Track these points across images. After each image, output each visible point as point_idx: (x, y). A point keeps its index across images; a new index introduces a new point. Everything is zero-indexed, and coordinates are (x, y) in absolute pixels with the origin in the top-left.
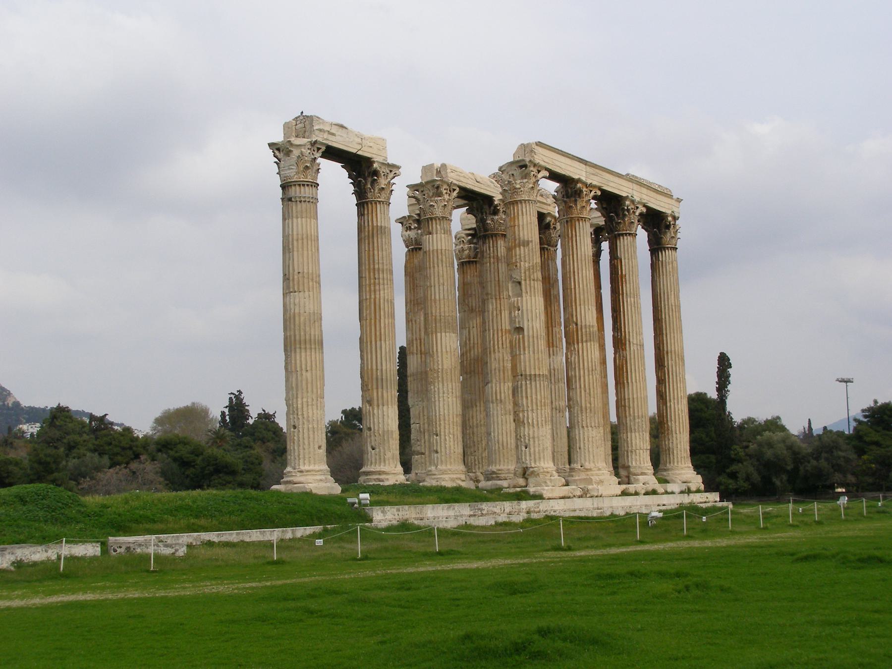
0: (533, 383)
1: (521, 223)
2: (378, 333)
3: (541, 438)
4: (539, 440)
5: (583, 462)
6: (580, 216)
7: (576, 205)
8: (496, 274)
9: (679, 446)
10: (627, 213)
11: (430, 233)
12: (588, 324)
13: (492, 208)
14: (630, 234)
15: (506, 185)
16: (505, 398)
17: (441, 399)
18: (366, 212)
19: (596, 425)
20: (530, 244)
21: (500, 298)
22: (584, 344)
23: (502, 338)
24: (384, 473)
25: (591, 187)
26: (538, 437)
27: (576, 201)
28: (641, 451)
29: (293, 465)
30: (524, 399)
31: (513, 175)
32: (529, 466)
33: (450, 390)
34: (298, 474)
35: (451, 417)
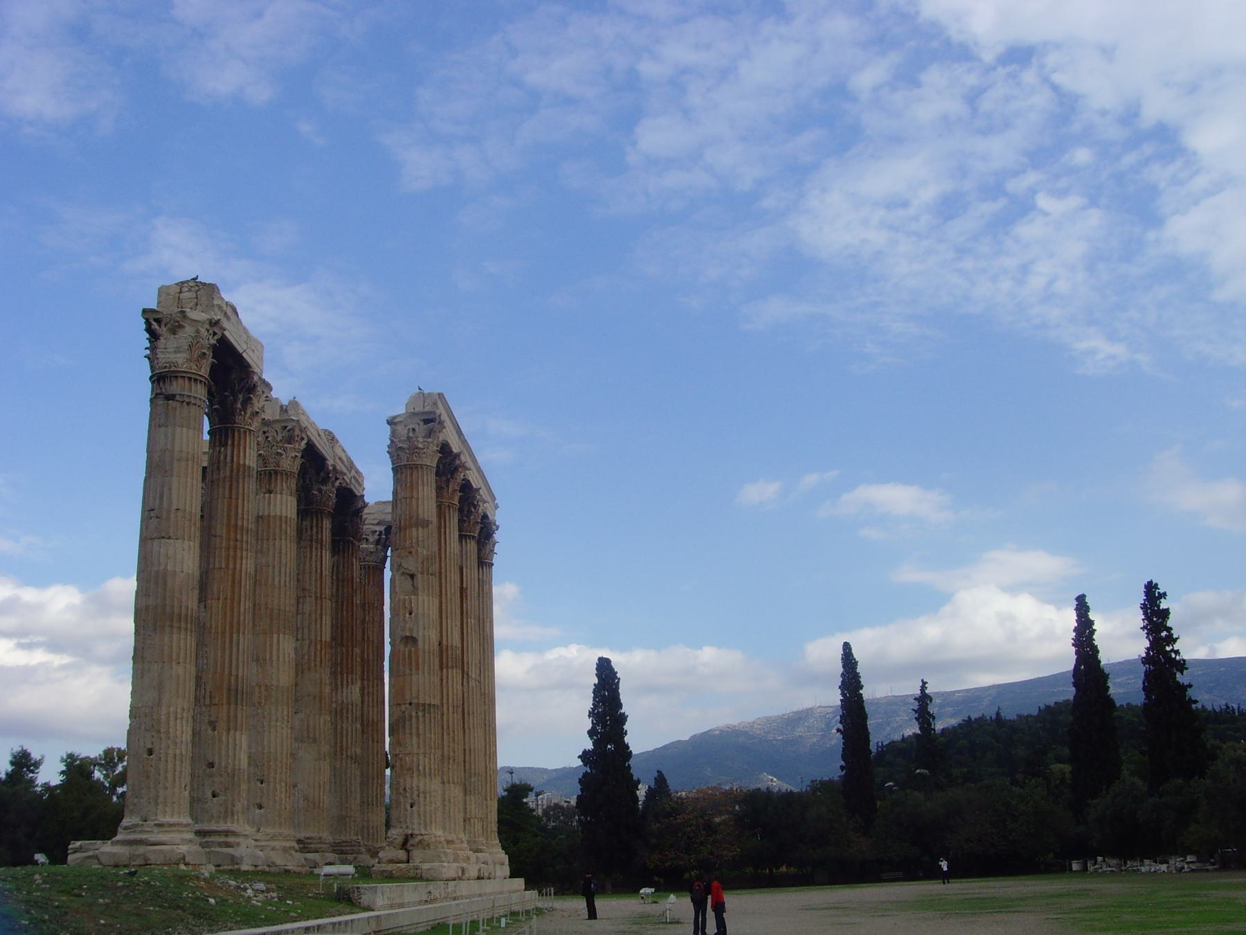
0: (427, 715)
1: (420, 496)
4: (431, 797)
7: (448, 486)
8: (319, 563)
10: (473, 510)
11: (270, 492)
13: (322, 474)
15: (403, 442)
16: (320, 736)
18: (230, 442)
20: (430, 526)
21: (321, 598)
22: (450, 671)
24: (234, 833)
26: (430, 793)
30: (414, 738)
31: (414, 429)
32: (416, 832)
34: (156, 830)
35: (284, 755)
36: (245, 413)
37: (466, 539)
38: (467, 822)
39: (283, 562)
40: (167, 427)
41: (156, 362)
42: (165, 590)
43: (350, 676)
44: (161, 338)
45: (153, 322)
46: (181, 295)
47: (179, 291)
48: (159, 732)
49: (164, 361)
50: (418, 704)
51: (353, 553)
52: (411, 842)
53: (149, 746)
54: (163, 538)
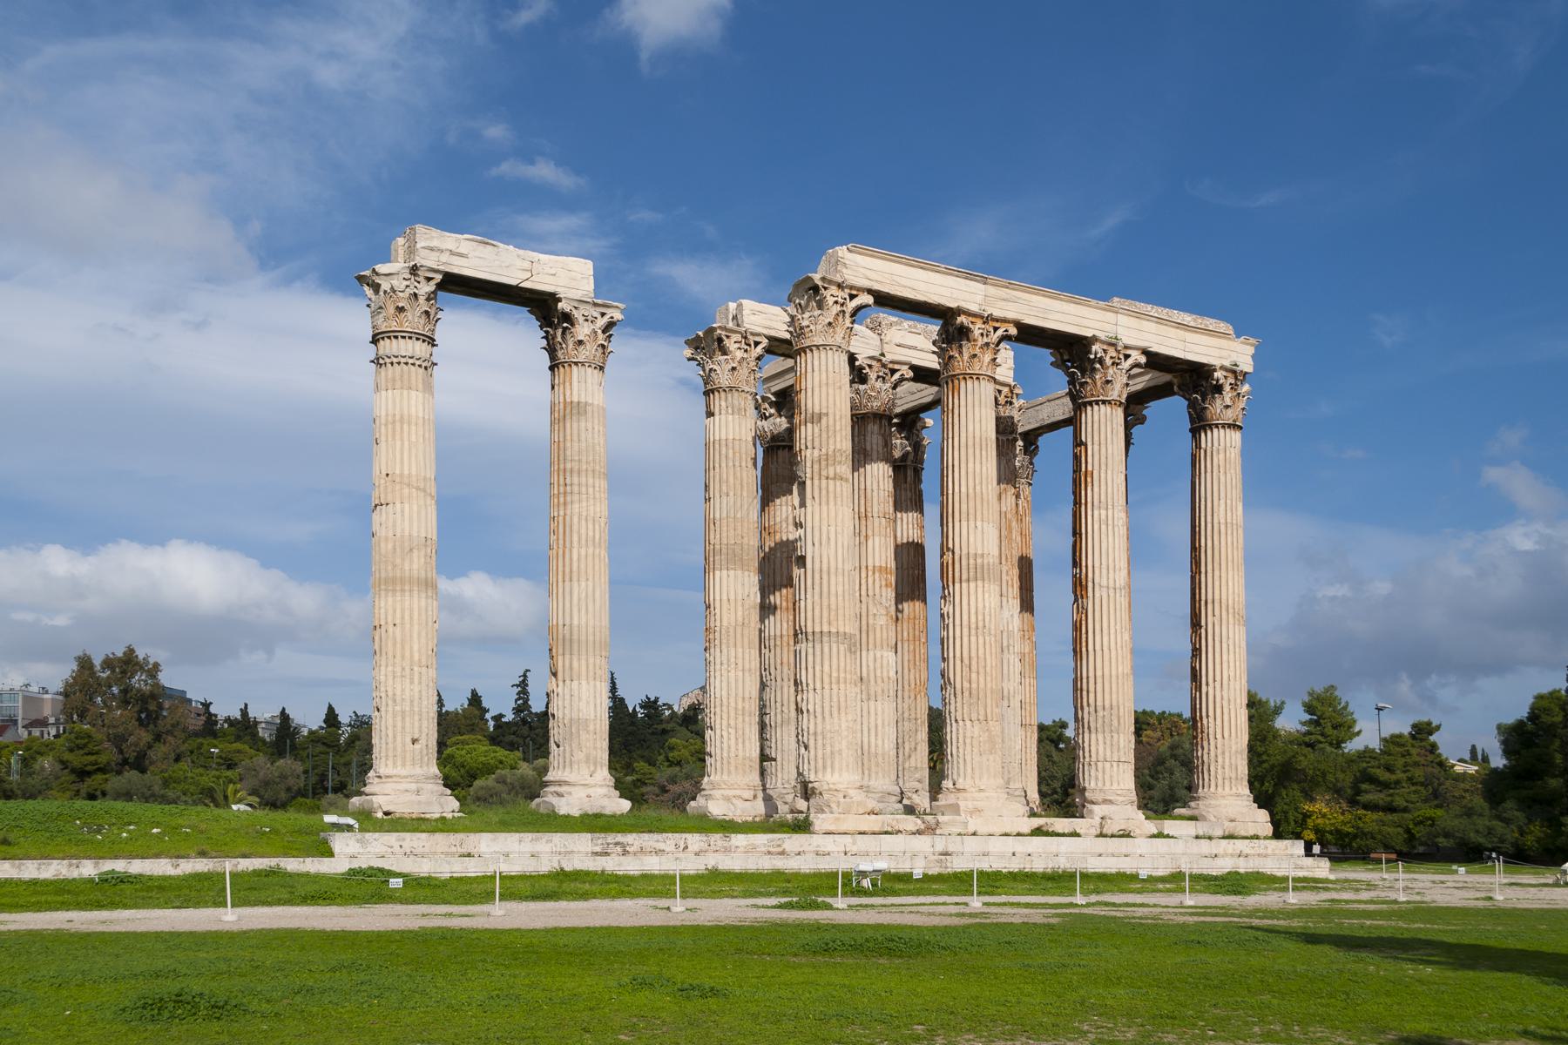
0: (818, 646)
2: (567, 570)
3: (829, 735)
5: (955, 777)
6: (968, 371)
7: (961, 353)
9: (1220, 760)
12: (972, 551)
14: (1104, 402)
17: (718, 674)
19: (981, 718)
22: (964, 585)
25: (997, 321)
27: (961, 346)
28: (1108, 765)
33: (733, 660)
37: (1092, 406)
38: (1093, 766)
39: (724, 488)
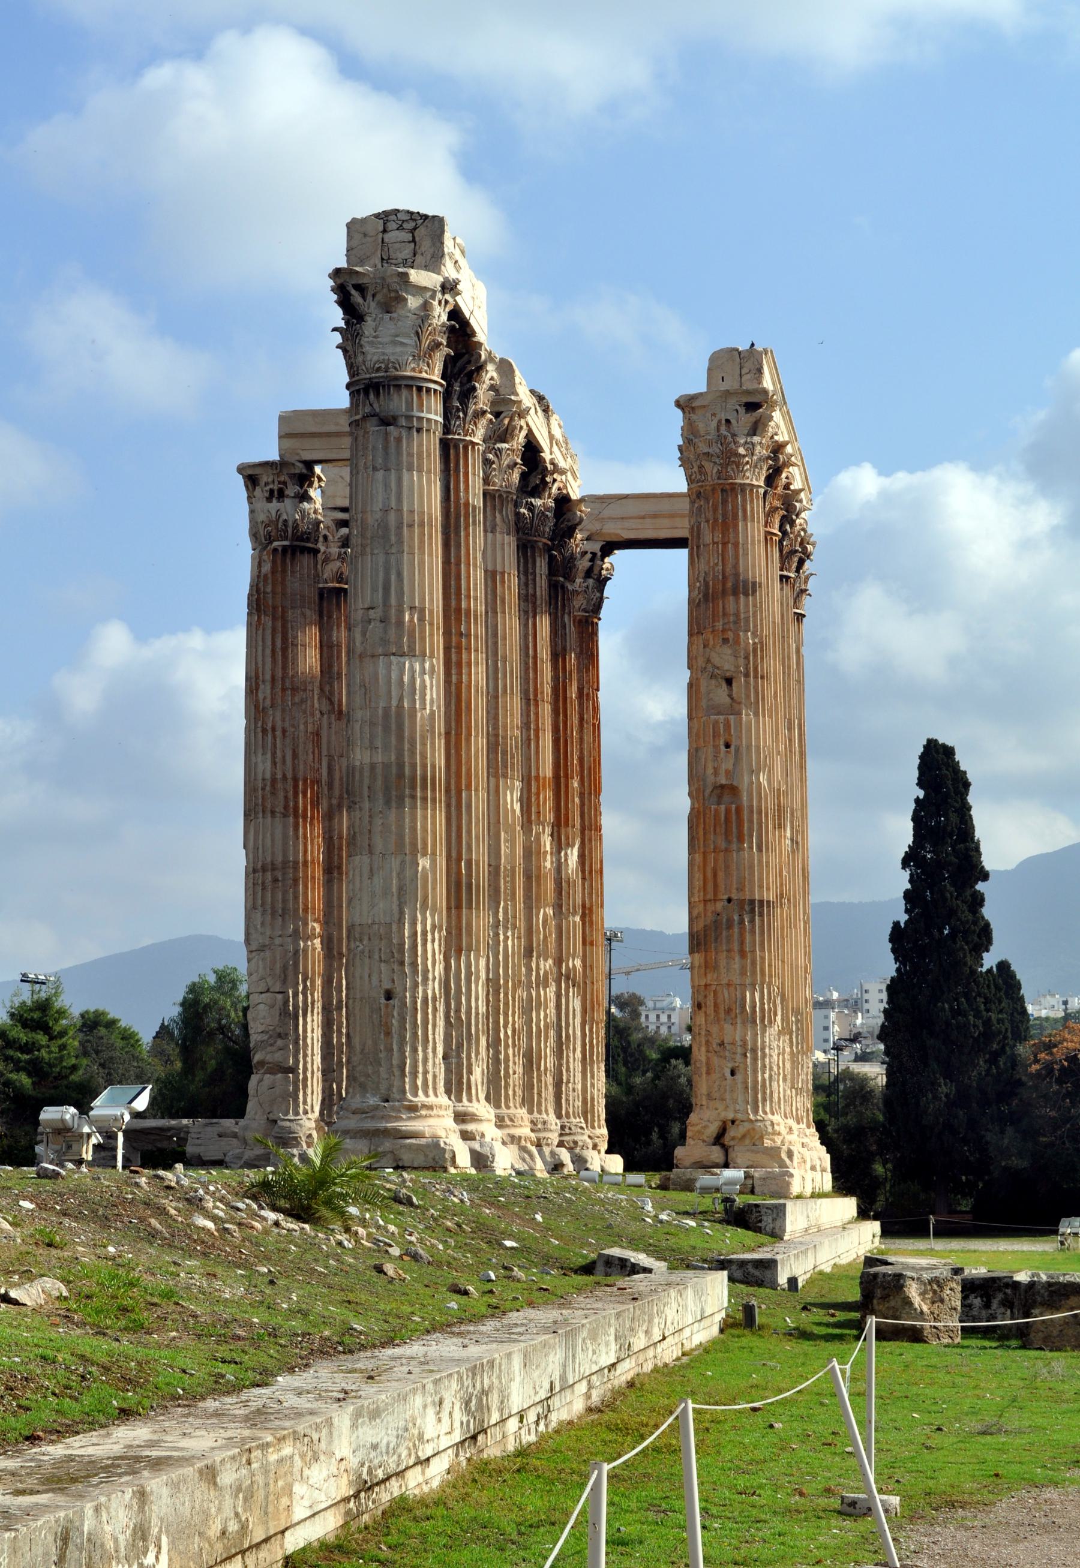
23: (538, 798)
29: (383, 1087)
32: (739, 1116)
36: (465, 414)
40: (387, 470)
41: (360, 358)
42: (400, 738)
43: (563, 830)
44: (368, 319)
45: (353, 292)
46: (387, 236)
47: (381, 229)
48: (402, 963)
49: (375, 358)
50: (741, 903)
51: (563, 606)
52: (732, 1132)
53: (387, 985)
54: (394, 654)
